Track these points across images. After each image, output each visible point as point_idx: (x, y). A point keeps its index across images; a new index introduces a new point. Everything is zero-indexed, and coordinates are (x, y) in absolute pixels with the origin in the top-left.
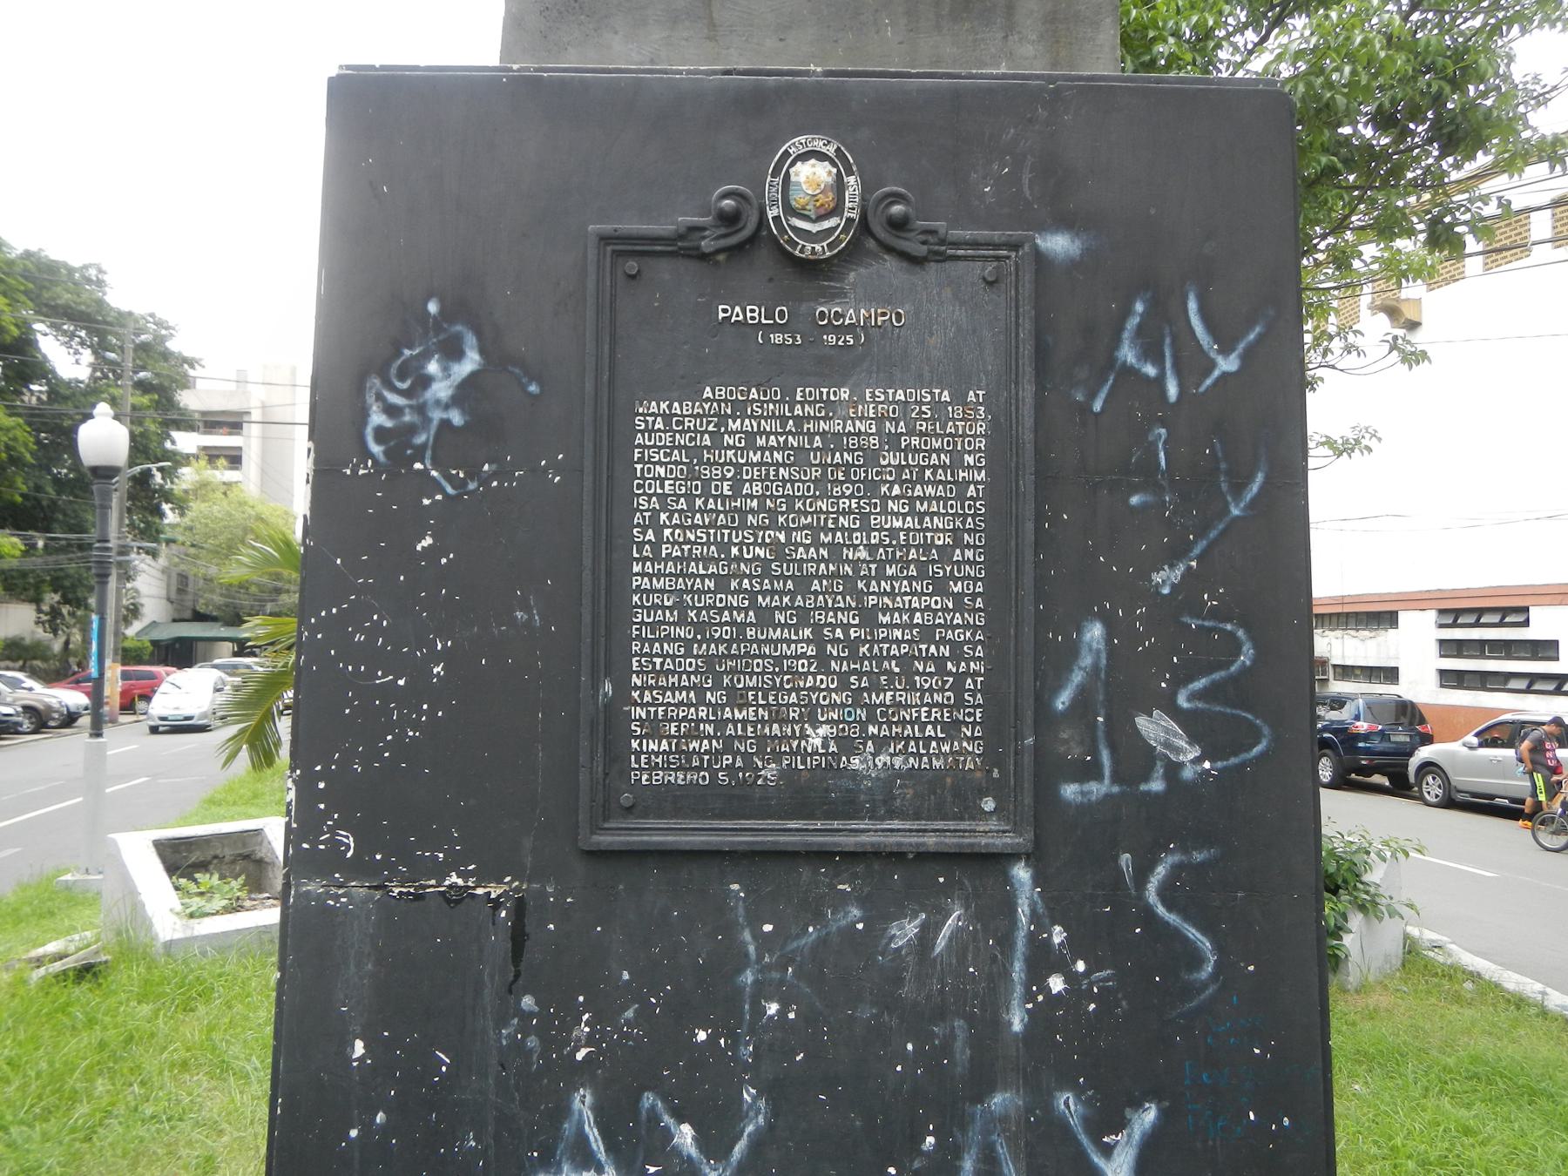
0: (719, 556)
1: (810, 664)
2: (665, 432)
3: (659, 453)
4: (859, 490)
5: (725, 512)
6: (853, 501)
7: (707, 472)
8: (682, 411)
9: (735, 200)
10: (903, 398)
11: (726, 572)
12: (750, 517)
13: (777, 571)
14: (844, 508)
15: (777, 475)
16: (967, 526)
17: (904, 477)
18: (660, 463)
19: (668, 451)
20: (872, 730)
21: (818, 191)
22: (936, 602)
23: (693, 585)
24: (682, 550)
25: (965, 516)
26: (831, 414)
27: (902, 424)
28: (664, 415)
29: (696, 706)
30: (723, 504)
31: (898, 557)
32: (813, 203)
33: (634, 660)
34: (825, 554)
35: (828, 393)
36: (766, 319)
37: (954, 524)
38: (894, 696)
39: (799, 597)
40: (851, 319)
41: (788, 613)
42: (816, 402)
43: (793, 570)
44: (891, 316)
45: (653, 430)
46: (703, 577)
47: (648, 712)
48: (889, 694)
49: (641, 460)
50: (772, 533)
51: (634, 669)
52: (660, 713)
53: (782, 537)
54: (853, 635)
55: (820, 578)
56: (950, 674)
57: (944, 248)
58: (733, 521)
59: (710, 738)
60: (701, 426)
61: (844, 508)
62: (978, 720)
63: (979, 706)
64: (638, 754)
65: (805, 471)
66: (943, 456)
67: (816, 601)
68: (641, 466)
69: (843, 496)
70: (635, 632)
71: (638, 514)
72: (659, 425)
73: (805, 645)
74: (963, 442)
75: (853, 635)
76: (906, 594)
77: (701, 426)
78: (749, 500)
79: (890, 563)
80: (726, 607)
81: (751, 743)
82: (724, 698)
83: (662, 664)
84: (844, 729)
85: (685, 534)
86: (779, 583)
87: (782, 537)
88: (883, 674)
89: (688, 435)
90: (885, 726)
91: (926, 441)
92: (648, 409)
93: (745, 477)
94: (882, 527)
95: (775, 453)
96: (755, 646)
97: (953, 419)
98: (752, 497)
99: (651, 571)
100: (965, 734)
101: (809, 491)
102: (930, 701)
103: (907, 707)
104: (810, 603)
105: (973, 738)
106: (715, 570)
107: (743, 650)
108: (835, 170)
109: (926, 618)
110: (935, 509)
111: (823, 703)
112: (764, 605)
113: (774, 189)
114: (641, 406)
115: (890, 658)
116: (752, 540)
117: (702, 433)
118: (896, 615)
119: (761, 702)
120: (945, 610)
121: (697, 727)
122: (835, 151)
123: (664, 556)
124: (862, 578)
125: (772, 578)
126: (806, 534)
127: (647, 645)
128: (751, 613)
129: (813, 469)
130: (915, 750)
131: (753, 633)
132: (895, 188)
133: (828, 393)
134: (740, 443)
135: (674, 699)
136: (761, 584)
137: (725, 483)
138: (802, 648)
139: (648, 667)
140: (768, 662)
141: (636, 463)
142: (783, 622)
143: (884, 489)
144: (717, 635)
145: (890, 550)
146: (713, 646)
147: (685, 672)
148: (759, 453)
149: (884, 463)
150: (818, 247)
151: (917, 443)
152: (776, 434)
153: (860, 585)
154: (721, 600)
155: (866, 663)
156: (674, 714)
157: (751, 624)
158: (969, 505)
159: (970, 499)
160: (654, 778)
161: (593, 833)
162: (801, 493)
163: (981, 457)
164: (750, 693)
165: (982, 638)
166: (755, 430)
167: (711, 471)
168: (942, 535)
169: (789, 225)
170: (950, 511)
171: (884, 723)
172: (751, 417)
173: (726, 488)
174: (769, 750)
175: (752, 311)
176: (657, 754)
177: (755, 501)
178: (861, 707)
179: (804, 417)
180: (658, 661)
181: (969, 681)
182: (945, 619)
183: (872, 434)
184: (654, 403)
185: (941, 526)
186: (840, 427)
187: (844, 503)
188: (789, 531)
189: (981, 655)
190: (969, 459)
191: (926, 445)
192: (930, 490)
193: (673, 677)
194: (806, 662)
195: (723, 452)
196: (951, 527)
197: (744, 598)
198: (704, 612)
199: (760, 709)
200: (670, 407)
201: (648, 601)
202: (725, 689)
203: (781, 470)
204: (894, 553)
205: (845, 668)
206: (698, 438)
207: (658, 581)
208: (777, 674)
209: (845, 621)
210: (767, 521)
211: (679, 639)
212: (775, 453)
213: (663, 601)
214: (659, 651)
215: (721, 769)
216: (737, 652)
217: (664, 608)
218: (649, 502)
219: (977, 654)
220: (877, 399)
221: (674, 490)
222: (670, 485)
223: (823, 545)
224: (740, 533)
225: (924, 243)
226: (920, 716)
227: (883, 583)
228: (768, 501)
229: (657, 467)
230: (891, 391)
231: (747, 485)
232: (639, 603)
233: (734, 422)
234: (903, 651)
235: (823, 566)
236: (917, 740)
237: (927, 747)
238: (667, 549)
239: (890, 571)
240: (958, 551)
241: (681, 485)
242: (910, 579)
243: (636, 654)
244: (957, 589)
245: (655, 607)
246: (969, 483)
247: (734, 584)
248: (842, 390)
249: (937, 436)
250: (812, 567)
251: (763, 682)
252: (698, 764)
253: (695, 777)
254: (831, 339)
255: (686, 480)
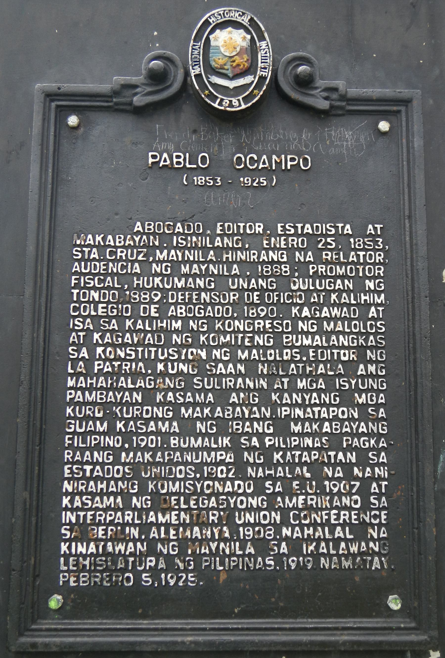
0: (146, 371)
1: (229, 471)
2: (99, 261)
3: (93, 280)
4: (272, 311)
5: (151, 332)
6: (267, 322)
7: (137, 296)
8: (115, 242)
9: (164, 63)
10: (310, 231)
11: (152, 386)
12: (175, 336)
13: (198, 385)
14: (259, 328)
15: (198, 299)
16: (369, 344)
17: (312, 300)
18: (94, 288)
19: (102, 277)
20: (286, 532)
21: (234, 53)
22: (343, 412)
23: (122, 398)
24: (113, 366)
25: (368, 334)
26: (247, 246)
27: (310, 253)
28: (98, 247)
29: (122, 511)
30: (151, 325)
31: (308, 372)
32: (229, 63)
33: (66, 467)
34: (243, 369)
35: (245, 227)
36: (190, 164)
37: (358, 342)
38: (305, 500)
39: (219, 409)
40: (264, 163)
41: (209, 423)
42: (233, 235)
43: (213, 383)
44: (299, 161)
45: (89, 260)
46: (131, 391)
47: (78, 517)
48: (301, 498)
49: (77, 286)
50: (194, 351)
51: (66, 476)
52: (89, 517)
53: (203, 355)
54: (268, 444)
55: (238, 391)
56: (356, 478)
57: (344, 104)
58: (159, 340)
59: (135, 541)
60: (132, 256)
61: (259, 328)
62: (384, 522)
63: (384, 508)
64: (67, 556)
65: (224, 295)
66: (346, 282)
67: (233, 412)
68: (78, 291)
69: (258, 317)
70: (67, 442)
71: (74, 334)
72: (95, 254)
73: (223, 453)
74: (364, 269)
75: (268, 444)
76: (315, 405)
77: (132, 256)
78: (173, 322)
79: (301, 377)
80: (152, 418)
81: (173, 546)
82: (149, 502)
83: (92, 471)
84: (259, 532)
85: (116, 352)
86: (200, 396)
87: (203, 355)
88: (294, 479)
89: (120, 264)
90: (297, 528)
91: (331, 268)
92: (85, 241)
93: (170, 301)
94: (293, 344)
95: (198, 280)
96: (178, 454)
97: (355, 250)
98: (176, 318)
99: (84, 385)
100: (371, 536)
101: (227, 313)
102: (338, 504)
103: (317, 510)
104: (228, 414)
105: (379, 539)
106: (142, 385)
107: (167, 458)
108: (249, 37)
109: (334, 427)
110: (341, 329)
111: (240, 507)
112: (186, 416)
113: (196, 52)
114: (79, 238)
115: (301, 464)
116: (176, 357)
117: (133, 262)
118: (307, 424)
119: (183, 506)
120: (351, 419)
121: (123, 531)
122: (249, 21)
123: (96, 371)
124: (276, 391)
125: (194, 392)
126: (225, 352)
127: (78, 453)
128: (175, 424)
129: (232, 294)
130: (325, 551)
131: (176, 442)
132: (301, 53)
133: (245, 227)
134: (166, 270)
135: (102, 503)
136: (184, 397)
137: (153, 306)
138: (221, 455)
139: (78, 474)
140: (190, 469)
141: (74, 288)
142: (204, 431)
143: (295, 310)
144: (143, 444)
145: (301, 365)
146: (139, 454)
147: (113, 478)
148: (183, 279)
149: (294, 288)
150: (234, 100)
151: (323, 270)
152: (198, 262)
153: (274, 397)
154: (147, 411)
155: (280, 469)
156: (102, 518)
157: (174, 433)
158: (371, 325)
159: (373, 318)
160: (82, 579)
161: (21, 635)
162: (220, 315)
163: (380, 282)
164: (173, 498)
165: (385, 445)
166: (180, 259)
167: (140, 296)
168: (347, 352)
169: (210, 82)
170: (354, 330)
171: (296, 525)
172: (176, 248)
173: (153, 310)
174: (190, 552)
175: (178, 157)
176: (85, 557)
177: (180, 322)
178: (276, 511)
179: (223, 248)
180: (88, 468)
181: (374, 485)
182: (351, 428)
183: (284, 263)
184: (90, 236)
185: (346, 344)
186: (255, 257)
187: (259, 323)
188: (209, 349)
189: (385, 461)
190: (370, 284)
191: (331, 272)
192: (335, 312)
193: (102, 483)
194: (224, 468)
195: (151, 278)
196: (355, 344)
197: (168, 410)
198: (132, 423)
199: (182, 513)
200: (104, 239)
201: (80, 413)
202: (150, 494)
203: (203, 295)
204: (304, 368)
205: (260, 474)
206: (129, 266)
207: (90, 395)
208: (199, 480)
209: (261, 431)
210: (190, 340)
211: (108, 448)
212: (198, 280)
213: (94, 412)
214: (89, 459)
215: (145, 571)
216: (161, 460)
217: (95, 419)
218: (83, 323)
219: (381, 460)
220: (288, 232)
221: (107, 312)
222: (103, 308)
223: (241, 361)
224: (166, 351)
225: (326, 98)
226: (329, 519)
227: (294, 396)
228: (191, 322)
229: (92, 292)
230: (299, 226)
231: (173, 308)
232: (72, 415)
233: (161, 253)
234: (313, 458)
235: (240, 380)
236: (327, 541)
237: (336, 547)
238: (99, 365)
239: (301, 384)
240: (362, 366)
241: (113, 308)
242: (319, 391)
243: (68, 462)
244: (362, 400)
245: (87, 418)
246: (370, 305)
247: (159, 397)
248: (257, 224)
249: (341, 264)
250: (230, 381)
251: (185, 487)
252: (123, 566)
253: (120, 579)
254: (247, 181)
255: (117, 303)
